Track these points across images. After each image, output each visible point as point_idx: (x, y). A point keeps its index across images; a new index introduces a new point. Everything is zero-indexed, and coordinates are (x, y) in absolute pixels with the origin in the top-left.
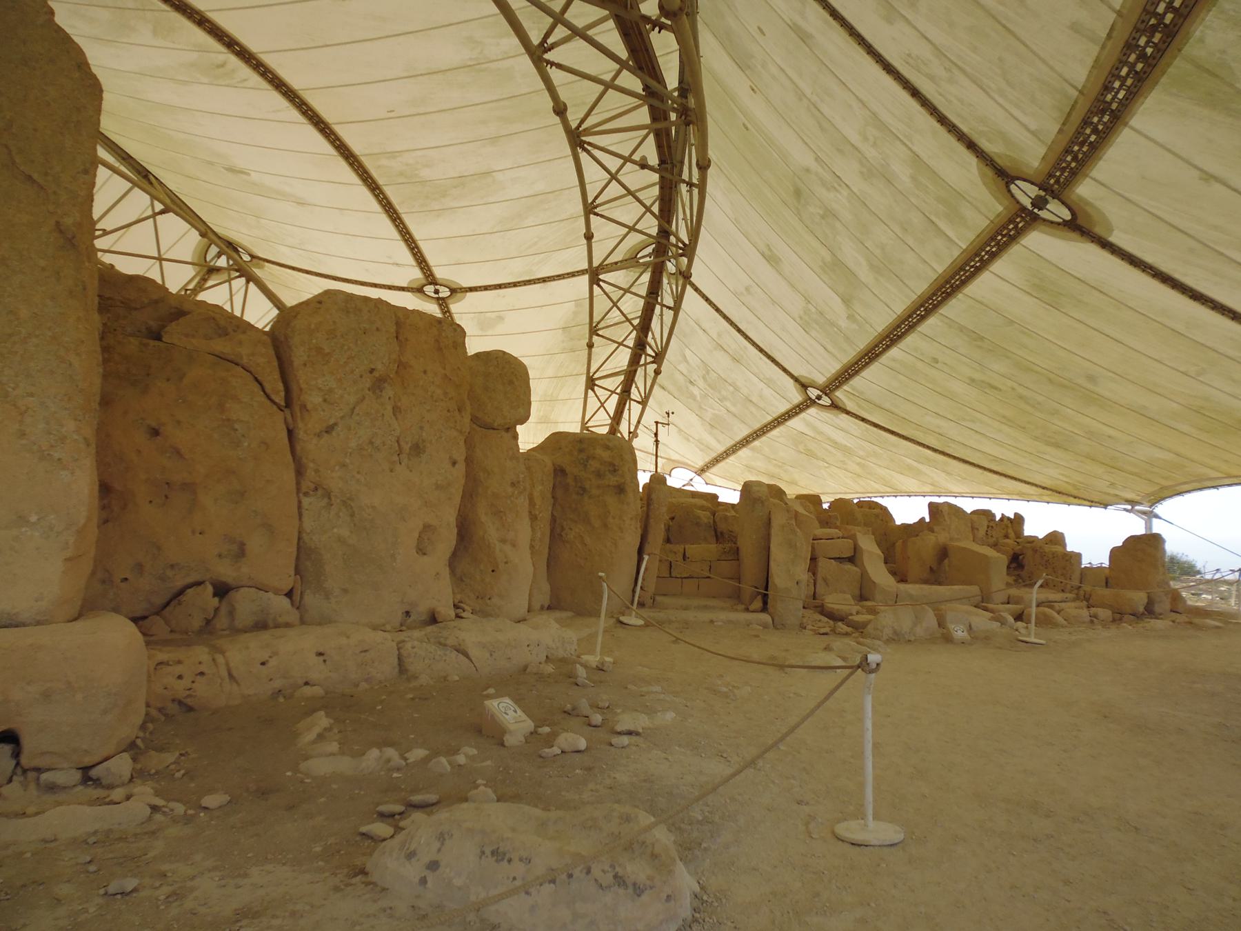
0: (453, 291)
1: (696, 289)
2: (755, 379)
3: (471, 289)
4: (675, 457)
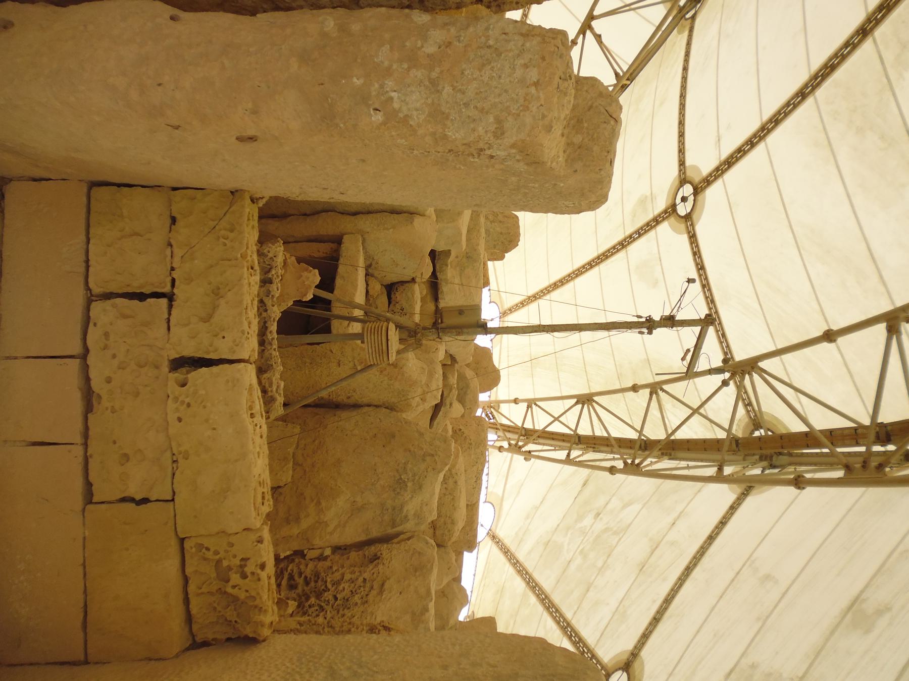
0: (688, 217)
1: (733, 509)
2: (620, 594)
3: (693, 238)
4: (506, 505)
